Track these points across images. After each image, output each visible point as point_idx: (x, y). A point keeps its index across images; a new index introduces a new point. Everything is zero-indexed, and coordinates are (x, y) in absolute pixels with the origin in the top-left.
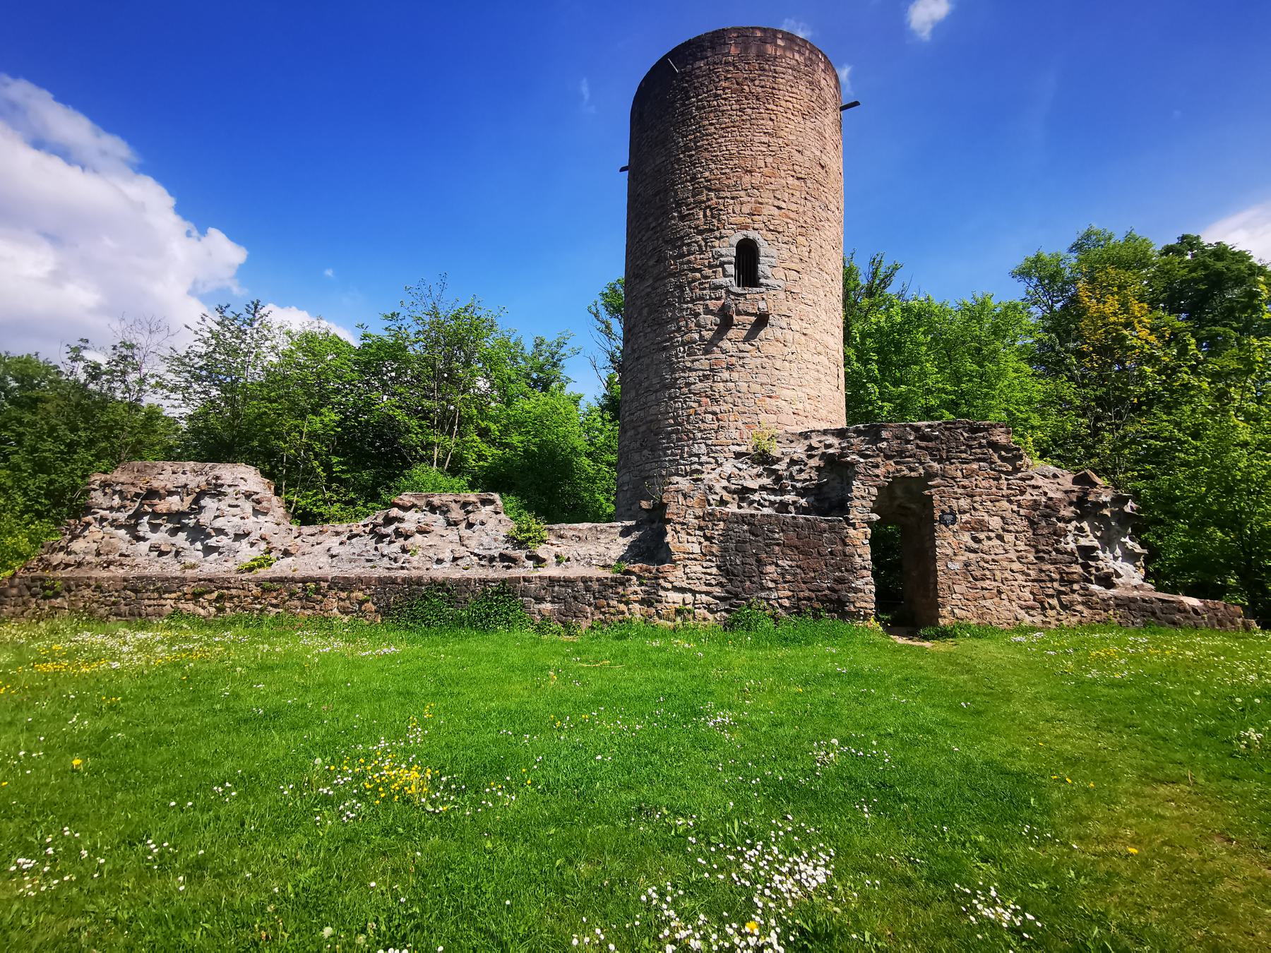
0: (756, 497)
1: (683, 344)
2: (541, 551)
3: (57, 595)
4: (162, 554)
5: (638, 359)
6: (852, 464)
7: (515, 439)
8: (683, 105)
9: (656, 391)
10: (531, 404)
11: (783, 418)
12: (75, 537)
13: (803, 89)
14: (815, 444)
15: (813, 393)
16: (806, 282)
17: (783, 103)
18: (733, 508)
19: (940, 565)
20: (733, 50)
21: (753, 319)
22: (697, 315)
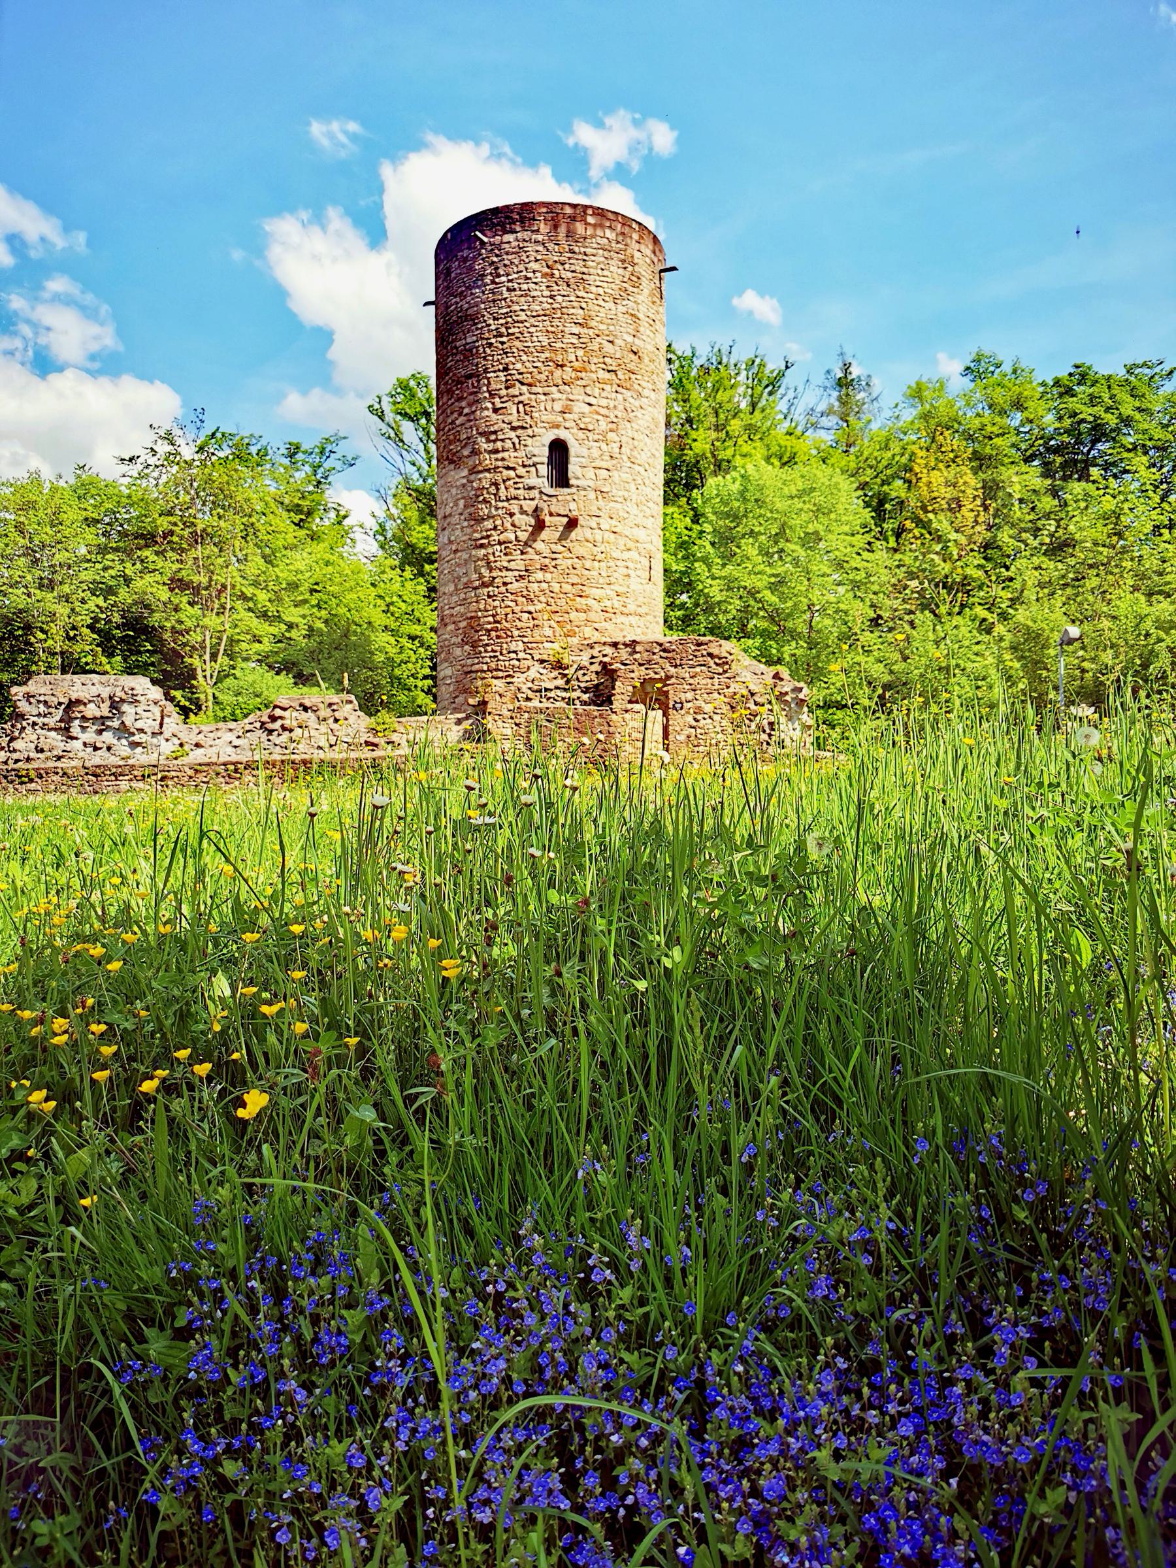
0: (551, 694)
1: (500, 543)
2: (395, 737)
3: (31, 781)
4: (96, 749)
5: (456, 551)
6: (615, 671)
7: (292, 614)
8: (493, 282)
9: (475, 588)
10: (301, 563)
11: (592, 616)
12: (13, 739)
13: (615, 269)
14: (595, 652)
15: (621, 589)
16: (616, 478)
17: (593, 289)
18: (535, 703)
20: (544, 228)
21: (565, 520)
22: (512, 515)
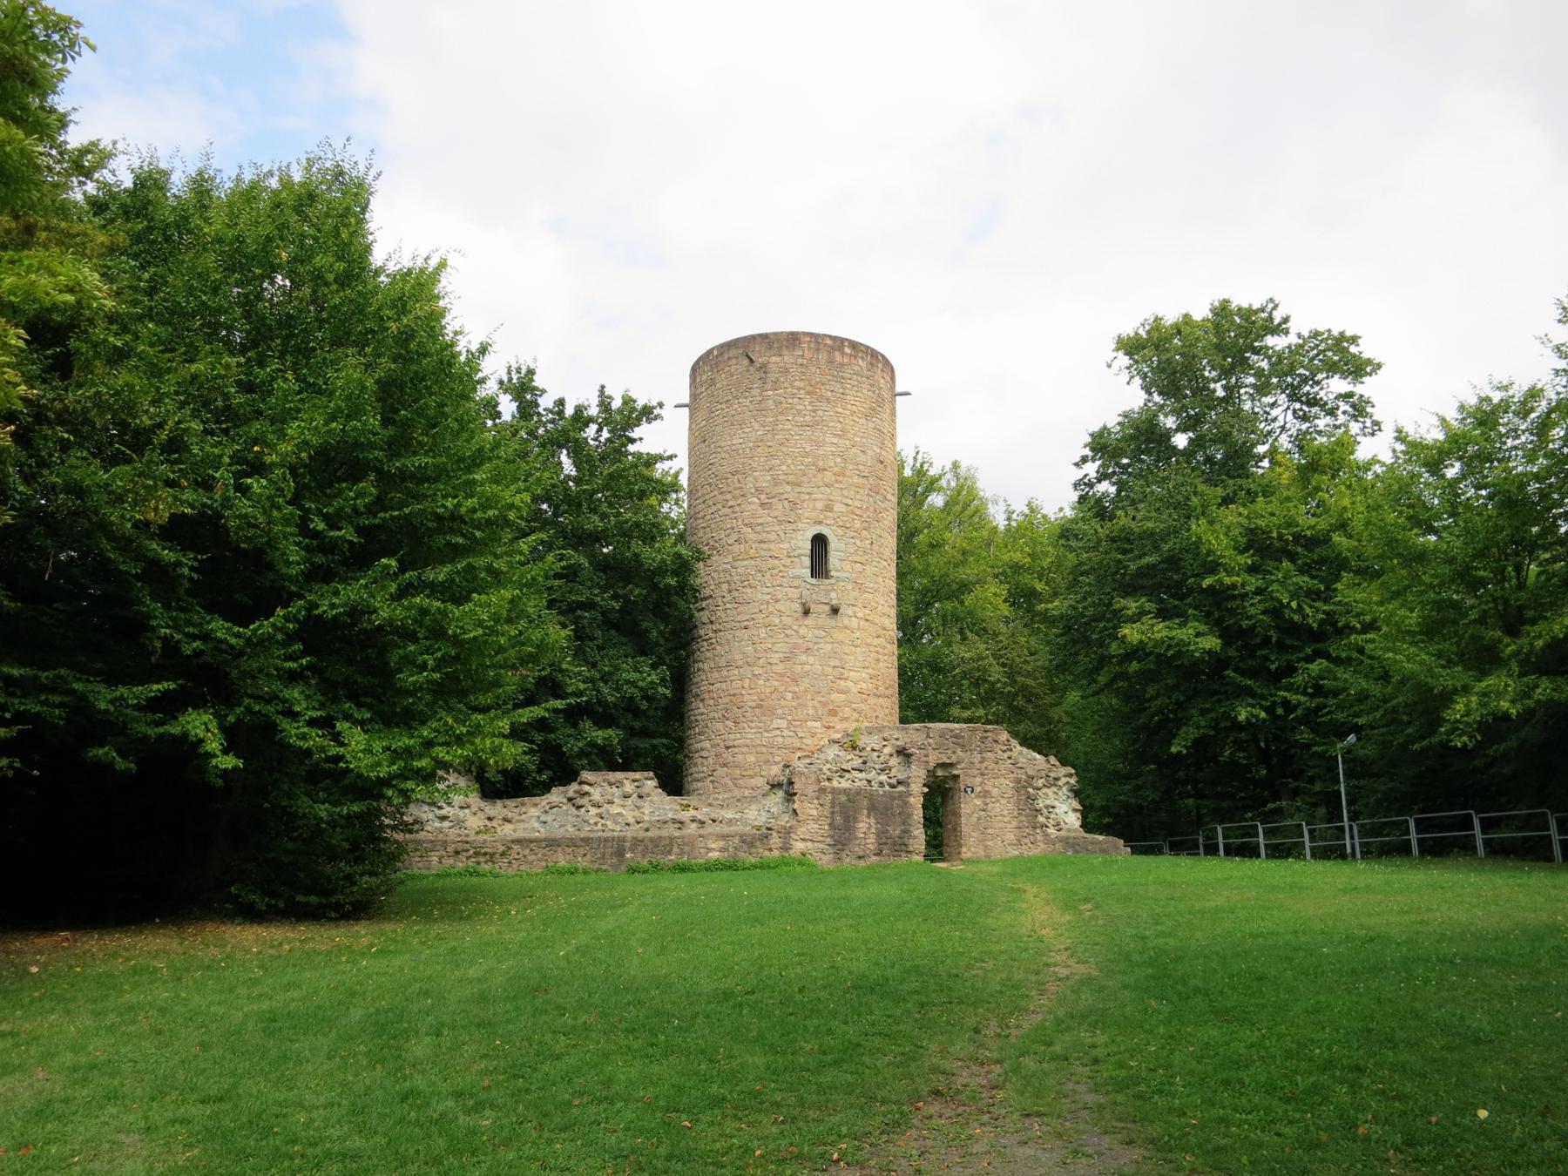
19: (963, 820)
21: (827, 608)
